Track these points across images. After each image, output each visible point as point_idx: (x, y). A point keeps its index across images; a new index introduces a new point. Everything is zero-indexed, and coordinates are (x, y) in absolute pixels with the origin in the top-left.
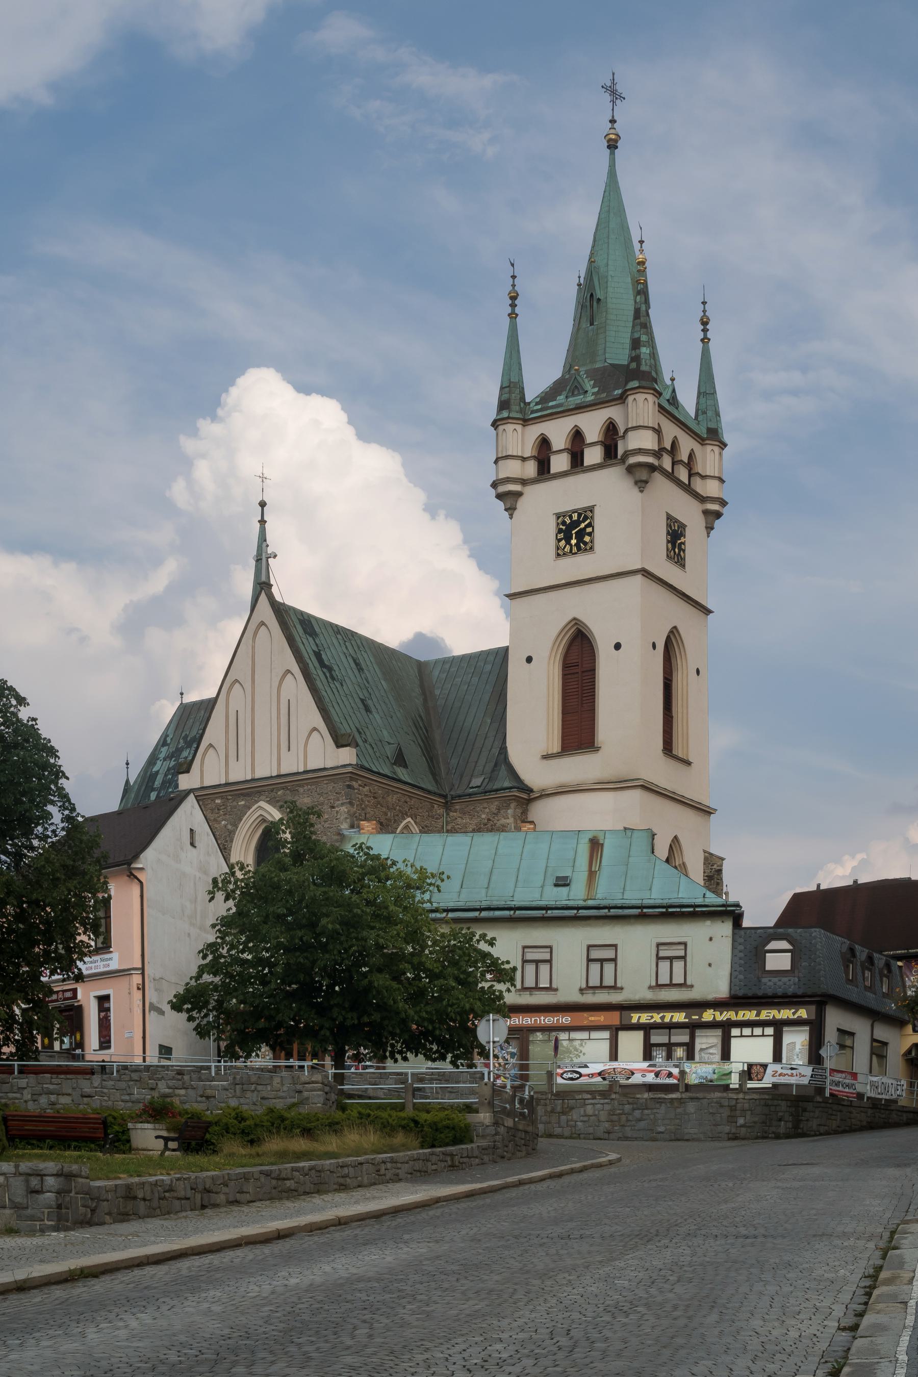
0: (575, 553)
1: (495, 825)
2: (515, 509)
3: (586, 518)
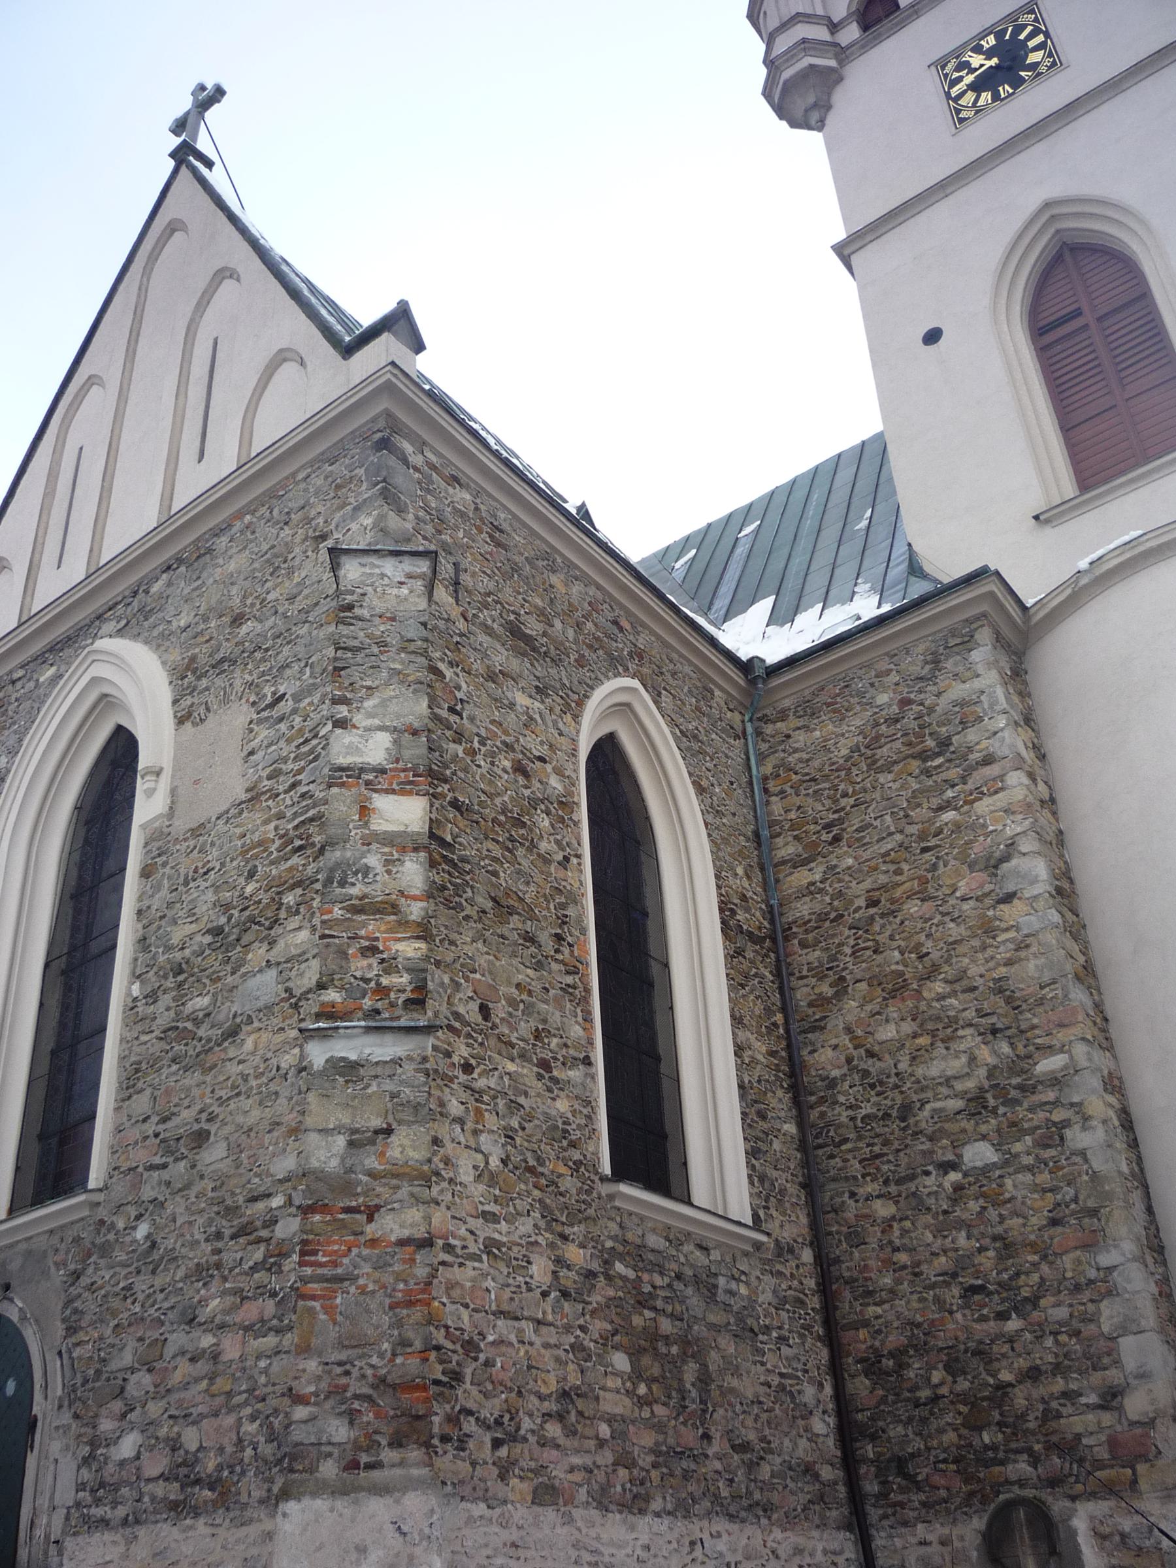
0: (1013, 94)
1: (931, 710)
2: (829, 107)
3: (1019, 29)
